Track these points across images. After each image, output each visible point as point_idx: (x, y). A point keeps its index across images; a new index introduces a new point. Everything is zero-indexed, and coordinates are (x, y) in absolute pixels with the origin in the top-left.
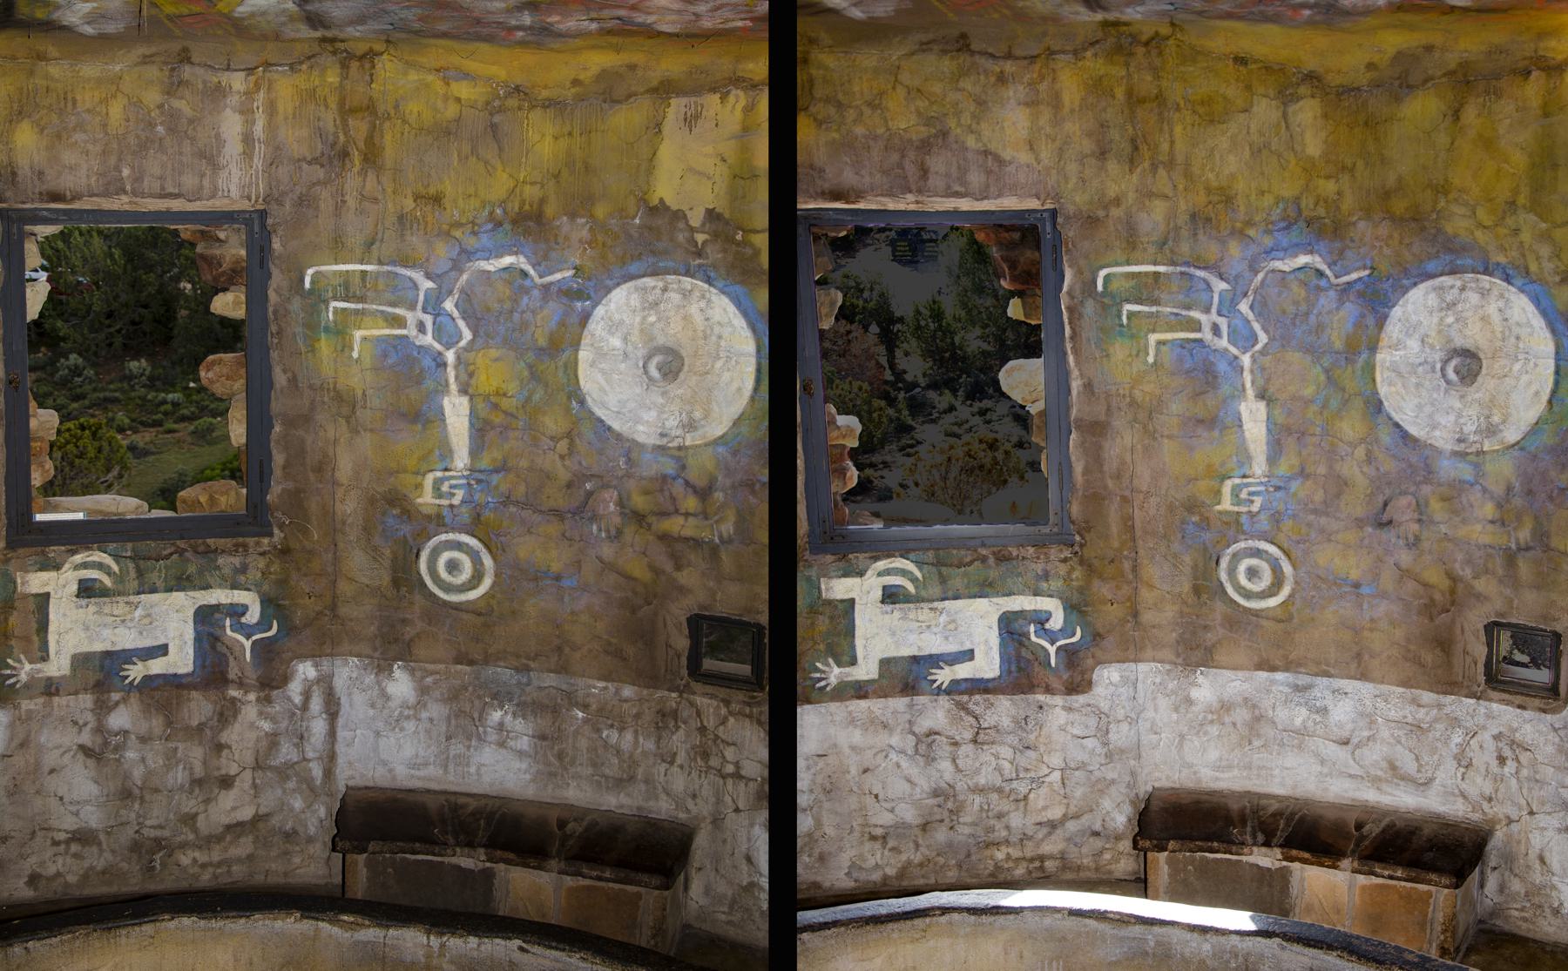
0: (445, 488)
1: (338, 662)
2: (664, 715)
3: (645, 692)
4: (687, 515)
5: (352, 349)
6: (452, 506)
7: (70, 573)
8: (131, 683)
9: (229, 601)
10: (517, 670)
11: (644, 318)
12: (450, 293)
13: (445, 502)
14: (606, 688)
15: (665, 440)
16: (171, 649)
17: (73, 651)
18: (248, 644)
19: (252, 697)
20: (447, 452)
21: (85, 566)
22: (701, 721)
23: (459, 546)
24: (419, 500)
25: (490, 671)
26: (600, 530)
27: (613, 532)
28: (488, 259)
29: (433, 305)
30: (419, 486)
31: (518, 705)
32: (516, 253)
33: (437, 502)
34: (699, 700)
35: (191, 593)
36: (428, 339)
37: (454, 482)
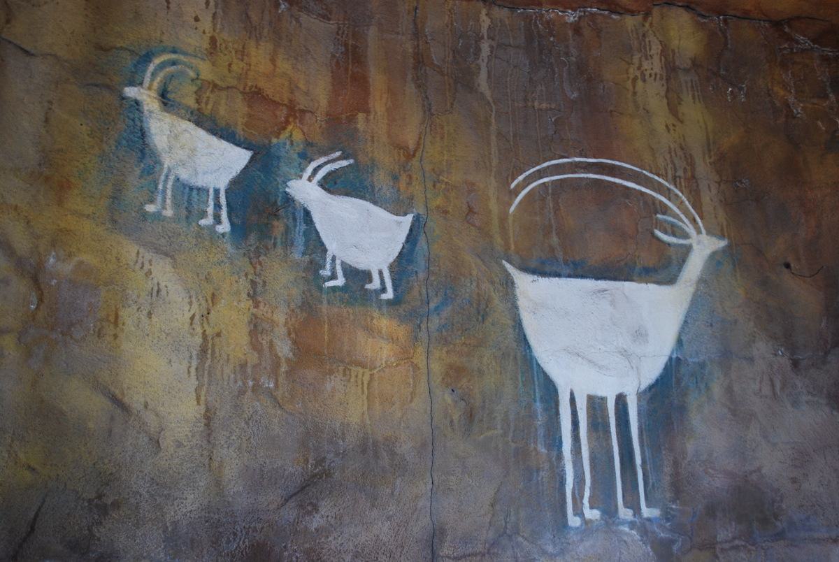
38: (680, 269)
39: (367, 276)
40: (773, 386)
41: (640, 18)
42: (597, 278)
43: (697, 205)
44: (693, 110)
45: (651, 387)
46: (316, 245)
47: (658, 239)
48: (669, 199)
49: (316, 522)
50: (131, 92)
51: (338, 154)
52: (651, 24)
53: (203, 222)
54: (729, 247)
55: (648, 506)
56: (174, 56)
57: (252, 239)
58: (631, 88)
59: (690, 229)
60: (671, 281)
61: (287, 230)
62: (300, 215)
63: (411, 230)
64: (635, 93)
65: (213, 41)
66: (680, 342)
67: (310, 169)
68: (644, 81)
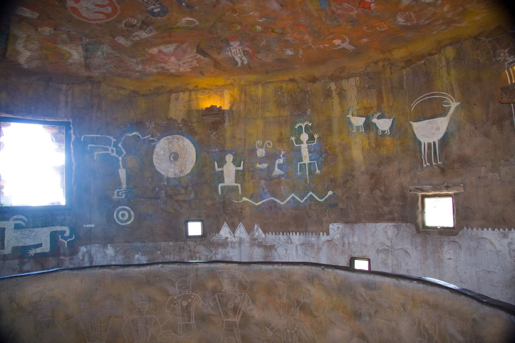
0: (120, 194)
1: (92, 246)
2: (180, 249)
3: (175, 243)
4: (182, 194)
5: (94, 157)
6: (122, 199)
7: (12, 222)
8: (31, 256)
9: (60, 230)
10: (142, 242)
11: (169, 146)
12: (120, 142)
13: (120, 198)
14: (165, 244)
15: (175, 176)
16: (43, 245)
17: (12, 246)
18: (66, 242)
19: (67, 258)
20: (120, 184)
21: (17, 219)
22: (190, 248)
23: (124, 209)
24: (113, 197)
25: (135, 244)
26: (161, 201)
27: (164, 201)
28: (129, 133)
29: (116, 145)
30: (113, 194)
31: (142, 252)
32: (136, 132)
33: (118, 198)
34: (189, 243)
35: (49, 228)
36: (114, 154)
37: (122, 192)
38: (448, 113)
39: (385, 131)
40: (470, 134)
41: (439, 54)
42: (430, 119)
43: (453, 96)
44: (453, 72)
45: (441, 139)
46: (377, 128)
47: (444, 107)
48: (446, 97)
49: (381, 169)
50: (348, 116)
51: (379, 112)
52: (442, 54)
53: (360, 131)
54: (461, 104)
55: (439, 162)
56: (352, 108)
57: (368, 131)
58: (438, 72)
59: (451, 102)
60: (445, 116)
61: (373, 127)
62: (374, 125)
63: (392, 121)
64: (439, 73)
65: (358, 102)
66: (447, 128)
67: (374, 117)
68: (441, 69)
